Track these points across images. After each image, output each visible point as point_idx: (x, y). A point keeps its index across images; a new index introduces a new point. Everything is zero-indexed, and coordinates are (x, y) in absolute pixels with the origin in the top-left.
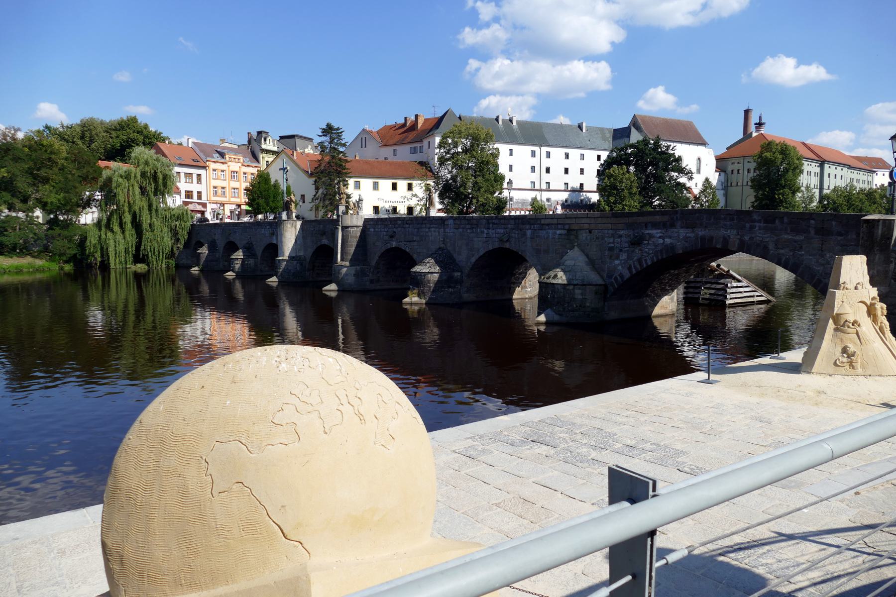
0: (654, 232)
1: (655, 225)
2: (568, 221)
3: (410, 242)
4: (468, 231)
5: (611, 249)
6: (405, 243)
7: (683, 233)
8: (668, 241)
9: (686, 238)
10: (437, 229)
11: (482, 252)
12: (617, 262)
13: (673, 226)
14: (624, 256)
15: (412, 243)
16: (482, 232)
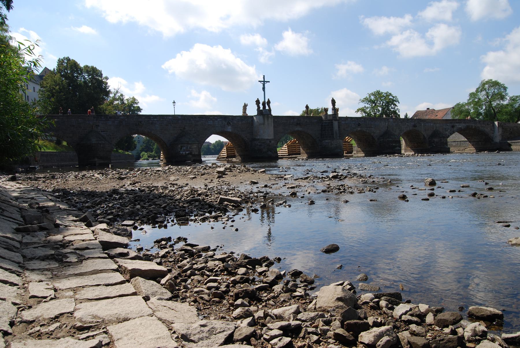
0: (457, 124)
1: (457, 123)
2: (434, 121)
3: (370, 128)
4: (400, 124)
5: (445, 129)
6: (366, 128)
7: (463, 125)
8: (460, 126)
9: (464, 126)
10: (385, 123)
11: (405, 131)
12: (447, 132)
13: (461, 123)
14: (449, 131)
15: (371, 128)
16: (406, 124)
